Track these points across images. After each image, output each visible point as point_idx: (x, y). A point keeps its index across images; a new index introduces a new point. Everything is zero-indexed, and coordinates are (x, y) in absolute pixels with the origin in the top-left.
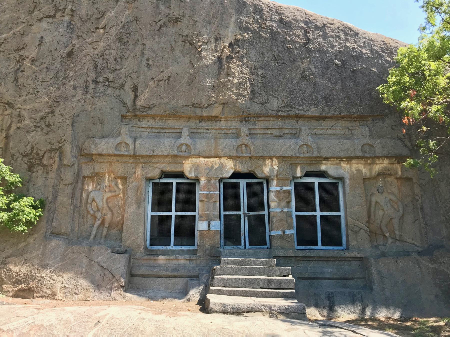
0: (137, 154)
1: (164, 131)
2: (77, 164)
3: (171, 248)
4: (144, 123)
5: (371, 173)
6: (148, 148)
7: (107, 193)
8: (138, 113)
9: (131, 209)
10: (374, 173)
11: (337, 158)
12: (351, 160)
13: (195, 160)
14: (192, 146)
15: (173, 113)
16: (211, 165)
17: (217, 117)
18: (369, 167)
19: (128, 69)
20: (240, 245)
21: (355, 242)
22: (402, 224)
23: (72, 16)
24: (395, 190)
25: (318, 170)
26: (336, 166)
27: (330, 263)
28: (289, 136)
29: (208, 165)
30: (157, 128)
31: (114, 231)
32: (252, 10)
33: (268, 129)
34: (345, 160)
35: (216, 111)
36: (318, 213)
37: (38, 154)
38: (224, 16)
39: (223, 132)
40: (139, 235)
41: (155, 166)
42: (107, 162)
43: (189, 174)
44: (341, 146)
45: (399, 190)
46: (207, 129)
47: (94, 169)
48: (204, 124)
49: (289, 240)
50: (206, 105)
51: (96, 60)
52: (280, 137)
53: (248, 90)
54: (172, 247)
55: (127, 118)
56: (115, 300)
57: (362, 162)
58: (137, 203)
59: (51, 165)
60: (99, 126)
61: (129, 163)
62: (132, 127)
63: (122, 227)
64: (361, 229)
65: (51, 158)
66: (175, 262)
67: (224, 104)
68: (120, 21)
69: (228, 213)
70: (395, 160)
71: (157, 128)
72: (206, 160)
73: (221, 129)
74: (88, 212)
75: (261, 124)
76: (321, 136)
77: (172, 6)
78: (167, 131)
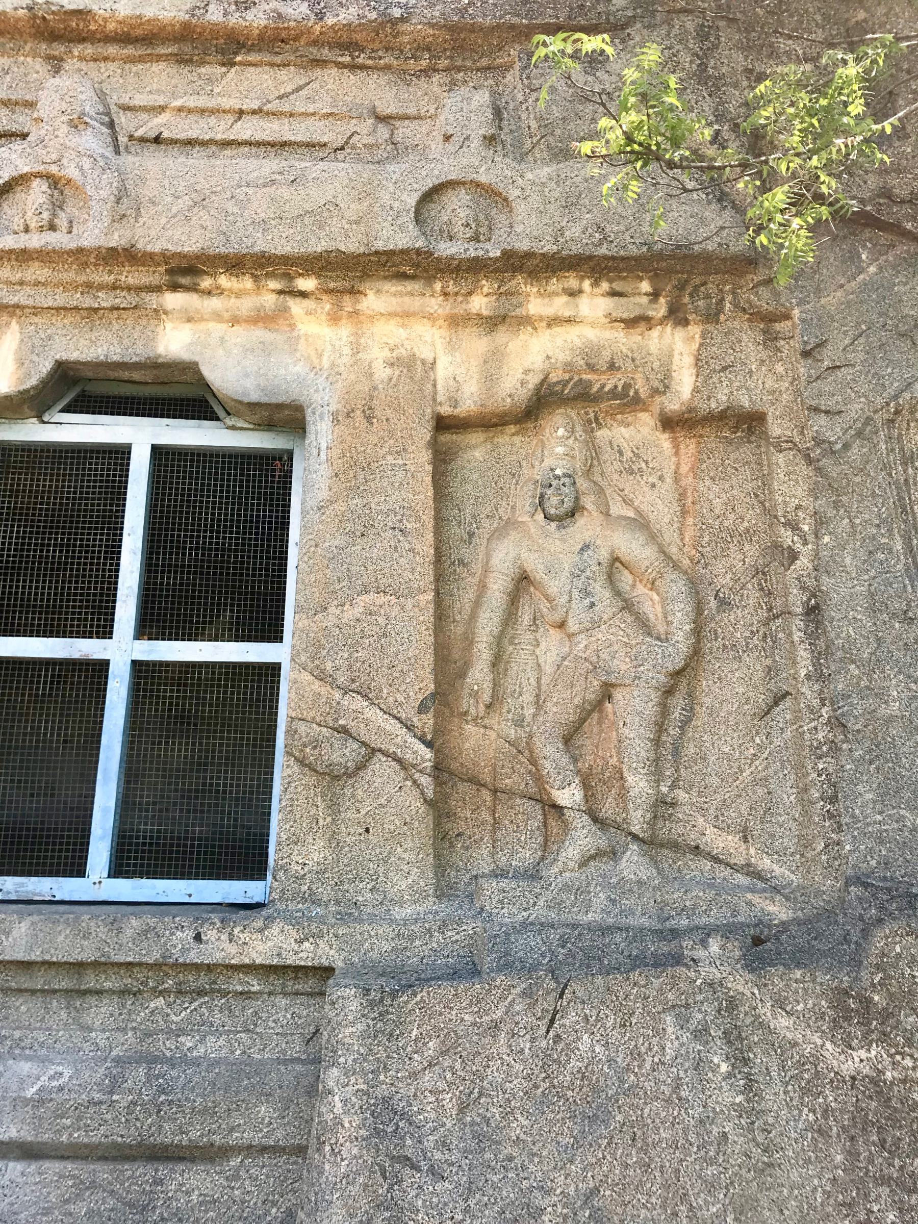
5: (489, 379)
21: (316, 852)
22: (685, 723)
24: (659, 506)
25: (137, 352)
26: (259, 333)
27: (100, 1013)
34: (307, 284)
44: (285, 192)
45: (682, 496)
57: (435, 304)
64: (374, 750)
70: (655, 295)
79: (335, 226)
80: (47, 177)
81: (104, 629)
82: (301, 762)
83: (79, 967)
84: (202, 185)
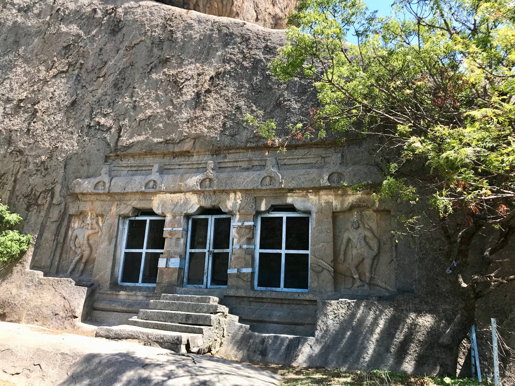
1: (141, 169)
2: (64, 203)
4: (124, 163)
5: (342, 205)
8: (119, 153)
10: (346, 205)
11: (303, 189)
12: (319, 192)
13: (162, 196)
17: (189, 152)
18: (341, 199)
19: (117, 112)
20: (202, 284)
21: (315, 284)
22: (377, 265)
23: (81, 69)
26: (303, 198)
27: (285, 306)
28: (259, 168)
29: (176, 200)
30: (135, 166)
32: (239, 40)
33: (237, 161)
34: (311, 191)
35: (187, 146)
36: (283, 251)
37: (35, 195)
38: (211, 51)
39: (194, 167)
44: (306, 176)
45: (378, 224)
46: (180, 165)
47: (79, 208)
48: (177, 160)
49: (245, 279)
50: (178, 141)
51: (93, 106)
52: (248, 169)
53: (220, 123)
54: (140, 284)
56: (66, 328)
57: (332, 193)
58: (109, 239)
59: (43, 205)
60: (86, 167)
61: (106, 201)
64: (323, 269)
65: (44, 198)
66: (134, 298)
67: (195, 139)
68: (118, 68)
69: (193, 251)
71: (135, 166)
72: (172, 195)
73: (193, 164)
74: (71, 248)
75: (231, 157)
76: (291, 166)
77: (164, 47)
78: (144, 169)
79: (315, 182)
80: (269, 176)
81: (281, 248)
82: (312, 270)
83: (282, 299)
84: (293, 176)
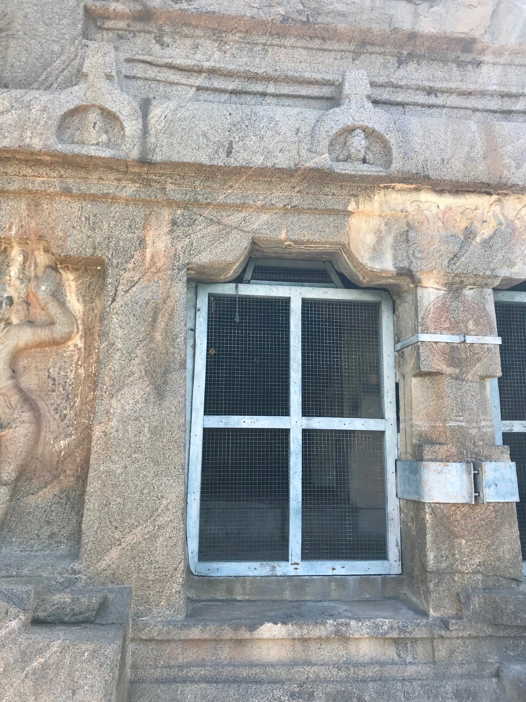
0: (158, 158)
1: (259, 88)
3: (292, 573)
6: (205, 135)
7: (13, 331)
9: (125, 403)
13: (400, 200)
14: (392, 139)
15: (300, 12)
16: (464, 224)
30: (229, 75)
31: (42, 498)
40: (161, 521)
41: (226, 220)
42: (18, 194)
43: (373, 259)
46: (431, 91)
55: (109, 24)
58: (150, 373)
62: (128, 61)
63: (82, 477)
71: (229, 75)
72: (447, 201)
78: (271, 89)
